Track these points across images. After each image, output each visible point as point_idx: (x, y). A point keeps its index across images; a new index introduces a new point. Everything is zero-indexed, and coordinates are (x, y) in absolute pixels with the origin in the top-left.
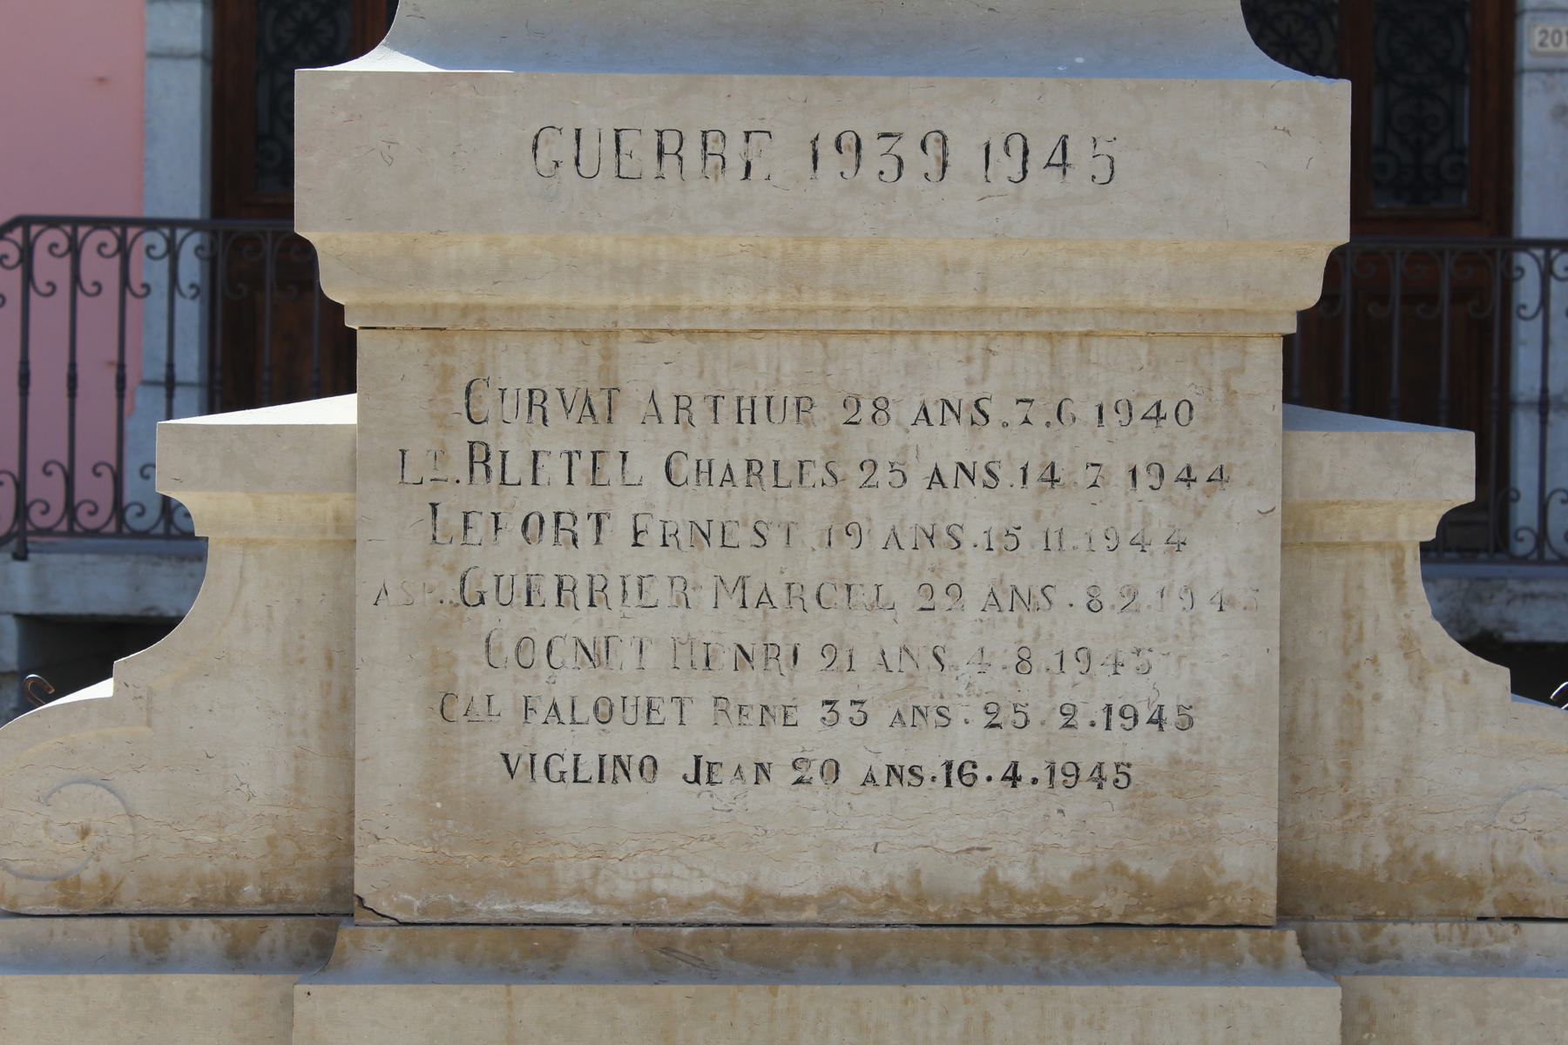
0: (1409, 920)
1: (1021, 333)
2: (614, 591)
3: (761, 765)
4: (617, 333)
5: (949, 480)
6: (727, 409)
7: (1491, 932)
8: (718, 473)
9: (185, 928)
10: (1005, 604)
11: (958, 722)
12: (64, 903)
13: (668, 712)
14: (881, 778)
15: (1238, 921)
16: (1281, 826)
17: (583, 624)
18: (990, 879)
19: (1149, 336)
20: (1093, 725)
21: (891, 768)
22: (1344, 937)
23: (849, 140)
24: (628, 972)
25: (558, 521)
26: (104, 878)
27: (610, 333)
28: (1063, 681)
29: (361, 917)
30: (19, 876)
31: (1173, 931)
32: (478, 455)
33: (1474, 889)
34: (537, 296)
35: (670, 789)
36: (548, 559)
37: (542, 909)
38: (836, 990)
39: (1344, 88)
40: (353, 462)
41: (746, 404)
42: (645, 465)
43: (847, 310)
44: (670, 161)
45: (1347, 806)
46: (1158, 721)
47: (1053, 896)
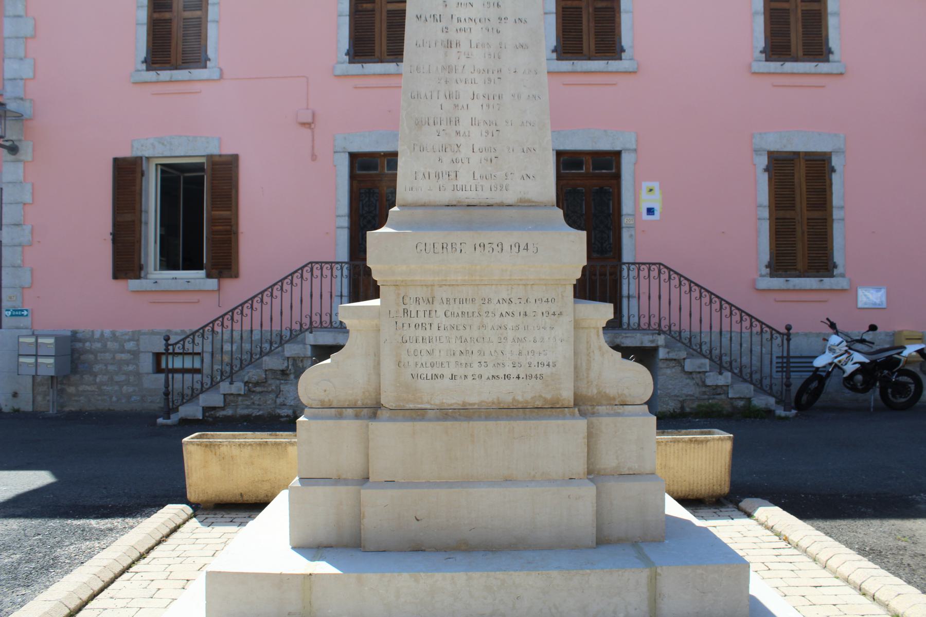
0: (601, 406)
2: (434, 339)
3: (465, 376)
4: (434, 285)
5: (504, 316)
6: (457, 301)
10: (516, 341)
11: (507, 366)
12: (321, 405)
13: (446, 365)
14: (491, 378)
15: (565, 406)
16: (574, 387)
17: (428, 347)
18: (514, 399)
19: (545, 285)
21: (493, 376)
22: (588, 409)
23: (482, 245)
24: (438, 419)
26: (329, 400)
27: (433, 285)
28: (528, 357)
30: (312, 400)
31: (552, 409)
32: (405, 312)
33: (614, 399)
34: (417, 278)
35: (446, 381)
36: (420, 333)
37: (420, 406)
38: (482, 422)
39: (585, 233)
41: (461, 300)
42: (441, 313)
43: (482, 280)
44: (445, 249)
45: (588, 382)
46: (548, 365)
47: (527, 402)
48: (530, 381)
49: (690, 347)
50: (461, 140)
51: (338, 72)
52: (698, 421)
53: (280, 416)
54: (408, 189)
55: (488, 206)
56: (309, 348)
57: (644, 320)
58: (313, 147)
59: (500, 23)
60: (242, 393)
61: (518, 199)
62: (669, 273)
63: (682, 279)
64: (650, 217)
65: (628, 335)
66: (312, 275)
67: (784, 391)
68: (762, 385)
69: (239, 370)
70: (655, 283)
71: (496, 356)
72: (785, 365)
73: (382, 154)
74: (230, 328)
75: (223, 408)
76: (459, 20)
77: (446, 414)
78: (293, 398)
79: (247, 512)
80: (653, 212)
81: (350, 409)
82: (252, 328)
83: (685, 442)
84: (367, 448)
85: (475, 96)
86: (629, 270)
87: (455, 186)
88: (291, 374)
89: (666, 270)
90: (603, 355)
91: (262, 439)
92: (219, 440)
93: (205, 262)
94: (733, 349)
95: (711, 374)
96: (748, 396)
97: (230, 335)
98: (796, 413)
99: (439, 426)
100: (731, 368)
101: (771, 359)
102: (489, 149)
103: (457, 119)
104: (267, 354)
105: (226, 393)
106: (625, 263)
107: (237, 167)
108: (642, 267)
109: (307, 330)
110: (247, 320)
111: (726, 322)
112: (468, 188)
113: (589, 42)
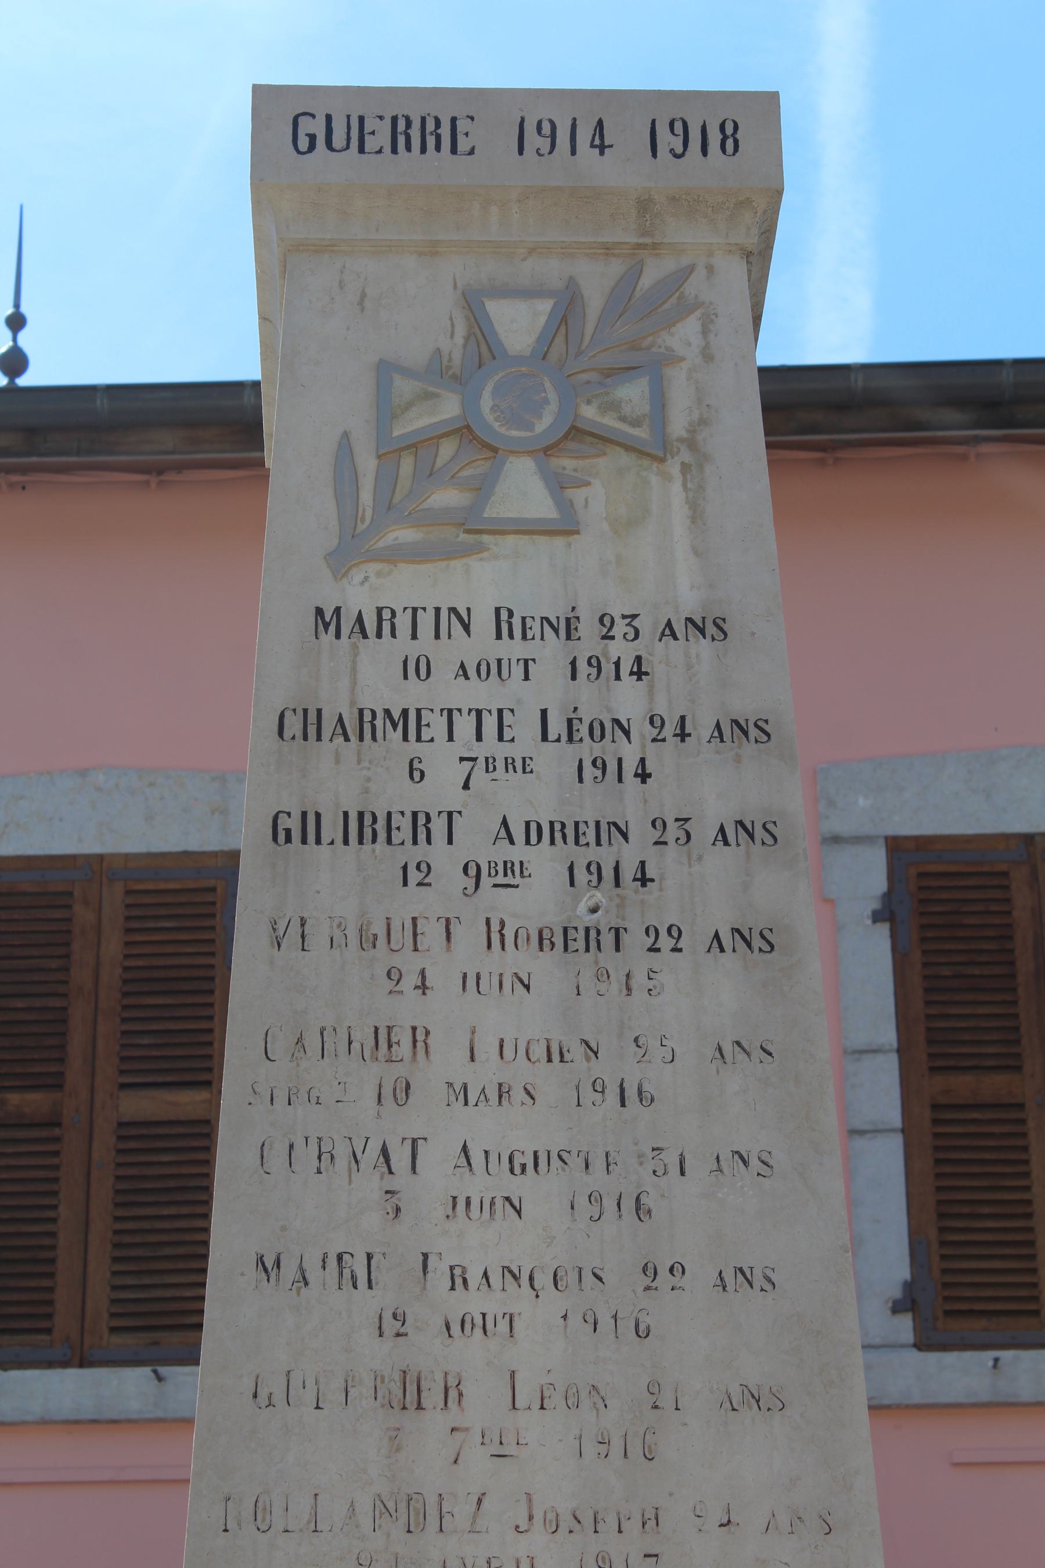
59: (648, 1288)
76: (458, 1279)
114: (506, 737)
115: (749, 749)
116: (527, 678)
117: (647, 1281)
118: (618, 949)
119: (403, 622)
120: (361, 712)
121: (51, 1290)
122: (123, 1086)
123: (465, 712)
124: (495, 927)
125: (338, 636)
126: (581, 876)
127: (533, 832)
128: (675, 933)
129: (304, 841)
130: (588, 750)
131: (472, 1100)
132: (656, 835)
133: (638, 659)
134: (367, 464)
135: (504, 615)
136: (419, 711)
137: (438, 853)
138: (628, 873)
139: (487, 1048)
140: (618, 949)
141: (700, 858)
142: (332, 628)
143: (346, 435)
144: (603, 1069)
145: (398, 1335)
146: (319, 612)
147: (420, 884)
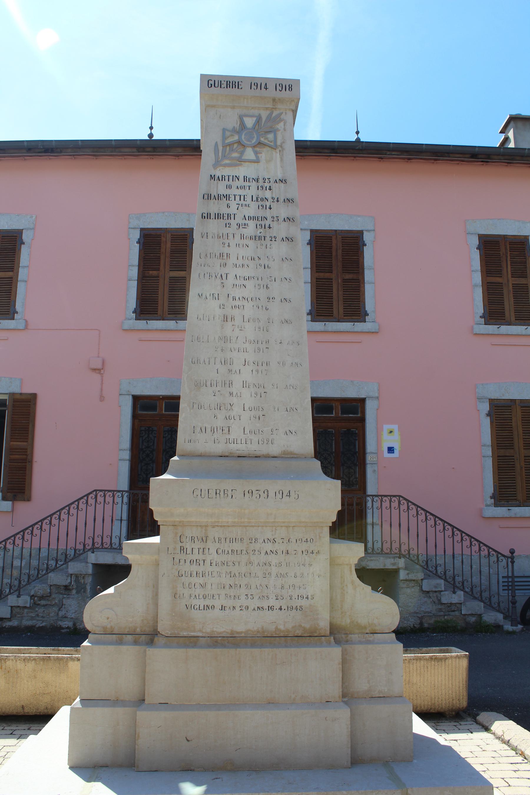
1: (282, 526)
2: (207, 574)
3: (234, 607)
4: (208, 526)
5: (269, 553)
6: (228, 540)
7: (368, 636)
8: (226, 552)
9: (126, 637)
10: (279, 576)
12: (104, 631)
13: (216, 597)
17: (201, 580)
19: (305, 527)
20: (295, 599)
21: (258, 607)
23: (250, 491)
24: (209, 646)
25: (196, 561)
26: (111, 627)
28: (290, 591)
29: (159, 635)
30: (96, 626)
31: (310, 637)
32: (182, 549)
33: (365, 628)
34: (193, 519)
35: (217, 611)
36: (194, 568)
37: (193, 634)
38: (248, 650)
40: (159, 550)
41: (231, 539)
42: (213, 551)
43: (250, 522)
44: (218, 495)
45: (342, 613)
48: (291, 611)
49: (427, 569)
50: (234, 400)
51: (126, 327)
52: (435, 636)
53: (61, 628)
54: (187, 441)
55: (256, 457)
56: (90, 566)
57: (387, 546)
58: (102, 390)
59: (268, 301)
60: (28, 605)
61: (282, 452)
62: (408, 504)
63: (419, 509)
64: (391, 455)
65: (372, 559)
66: (96, 501)
67: (510, 607)
68: (491, 603)
69: (26, 585)
70: (395, 513)
71: (262, 590)
72: (510, 584)
73: (161, 397)
74: (20, 546)
75: (9, 619)
76: (234, 299)
77: (216, 642)
78: (74, 611)
79: (27, 724)
80: (393, 450)
81: (130, 635)
82: (40, 547)
83: (426, 660)
84: (144, 671)
85: (247, 363)
86: (373, 501)
87: (228, 439)
88: (73, 589)
89: (404, 501)
90: (355, 589)
91: (45, 654)
92: (5, 655)
93: (1, 487)
94: (464, 570)
95: (446, 593)
96: (479, 613)
97: (21, 552)
98: (522, 628)
99: (210, 653)
100: (463, 588)
101: (498, 579)
102: (258, 407)
103: (231, 382)
104: (53, 570)
105: (13, 605)
106: (369, 496)
107: (35, 404)
108: (384, 499)
109: (89, 550)
110: (36, 540)
111: (458, 546)
112: (239, 442)
113: (338, 307)
114: (245, 200)
115: (290, 204)
116: (249, 189)
117: (268, 300)
118: (265, 240)
119: (227, 178)
120: (218, 195)
121: (157, 307)
122: (170, 270)
123: (238, 195)
124: (242, 235)
125: (214, 180)
126: (258, 226)
127: (250, 218)
128: (275, 238)
129: (208, 218)
130: (260, 203)
131: (237, 267)
132: (272, 219)
133: (270, 187)
134: (220, 148)
135: (245, 177)
136: (229, 195)
137: (232, 221)
138: (267, 226)
139: (240, 258)
140: (265, 240)
141: (280, 224)
142: (213, 179)
143: (217, 142)
144: (262, 262)
145: (223, 308)
146: (211, 176)
147: (229, 227)
